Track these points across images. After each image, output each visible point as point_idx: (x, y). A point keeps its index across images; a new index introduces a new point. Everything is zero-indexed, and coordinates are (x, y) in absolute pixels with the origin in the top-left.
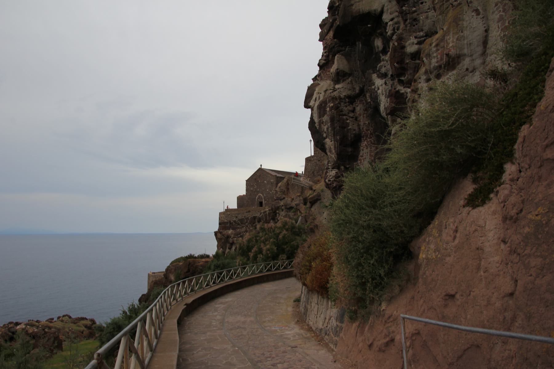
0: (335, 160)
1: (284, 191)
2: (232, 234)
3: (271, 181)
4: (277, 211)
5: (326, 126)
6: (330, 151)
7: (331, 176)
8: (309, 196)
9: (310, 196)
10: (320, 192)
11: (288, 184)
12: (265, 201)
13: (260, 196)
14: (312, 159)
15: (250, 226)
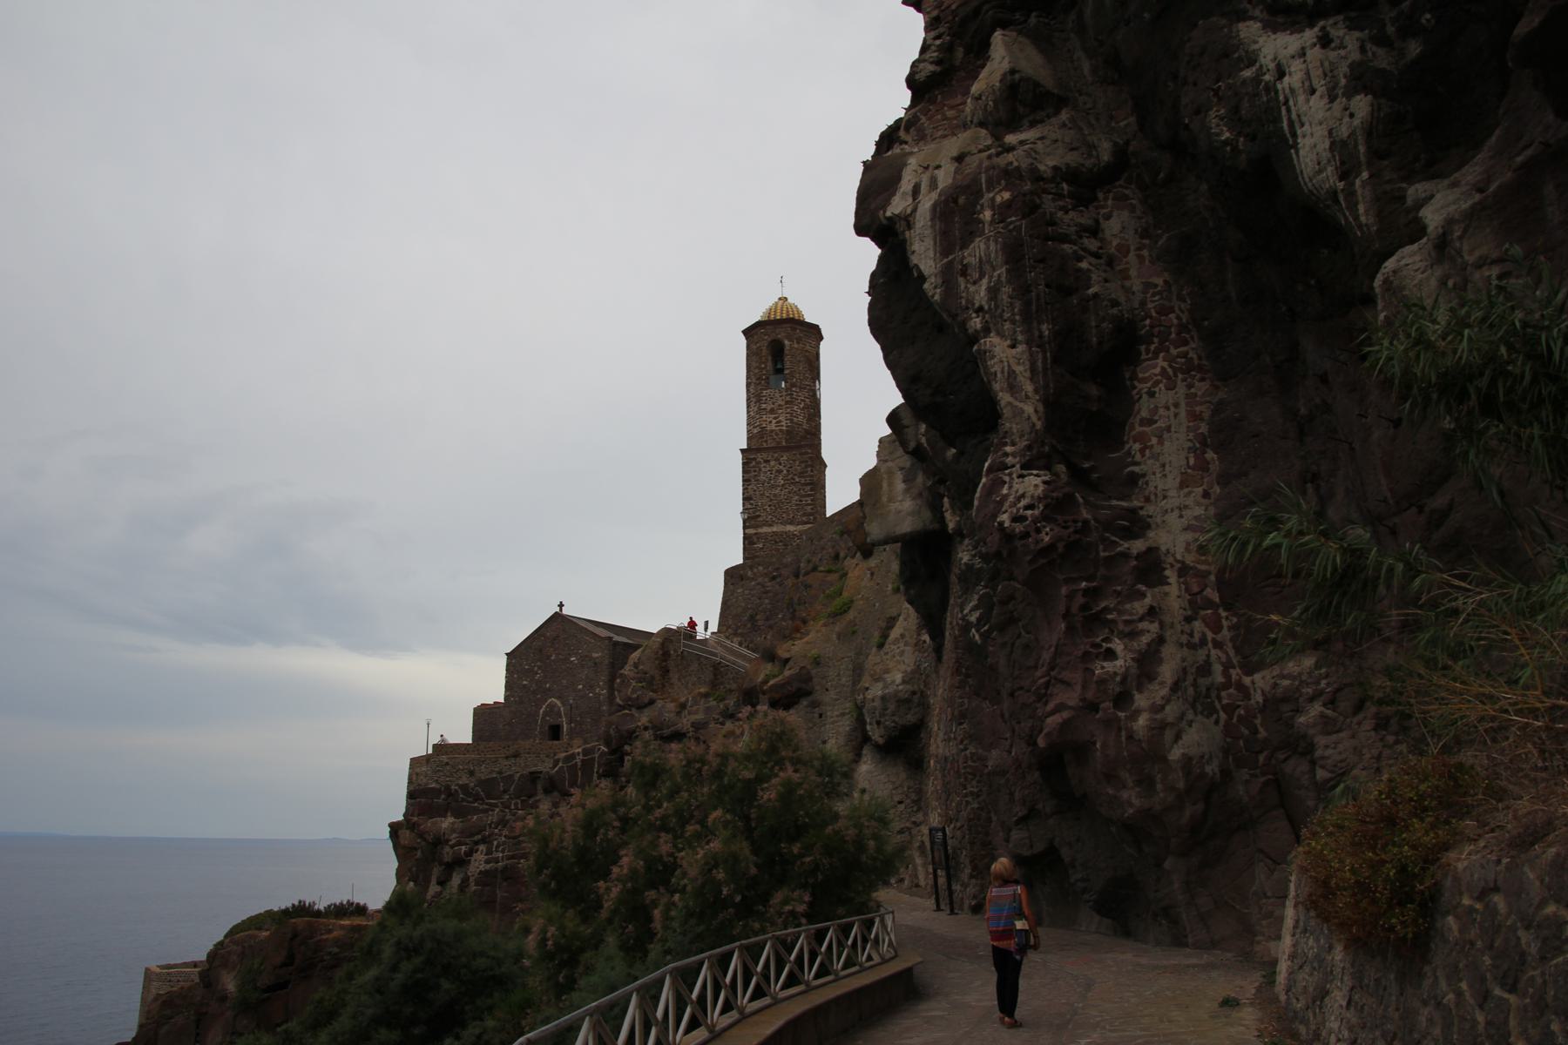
0: (1039, 425)
1: (653, 678)
2: (453, 831)
3: (595, 655)
4: (627, 748)
5: (985, 281)
6: (1013, 388)
7: (1023, 496)
8: (765, 682)
9: (771, 682)
10: (809, 667)
11: (666, 655)
12: (570, 722)
13: (552, 706)
14: (750, 573)
15: (516, 804)
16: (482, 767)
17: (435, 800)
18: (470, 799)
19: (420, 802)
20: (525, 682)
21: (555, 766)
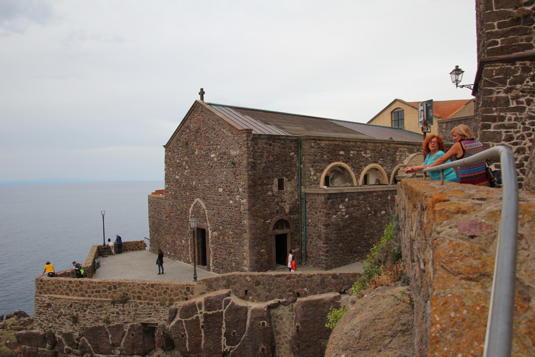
3: (233, 153)
16: (87, 313)
17: (40, 349)
18: (78, 351)
19: (25, 349)
20: (177, 177)
21: (171, 319)
